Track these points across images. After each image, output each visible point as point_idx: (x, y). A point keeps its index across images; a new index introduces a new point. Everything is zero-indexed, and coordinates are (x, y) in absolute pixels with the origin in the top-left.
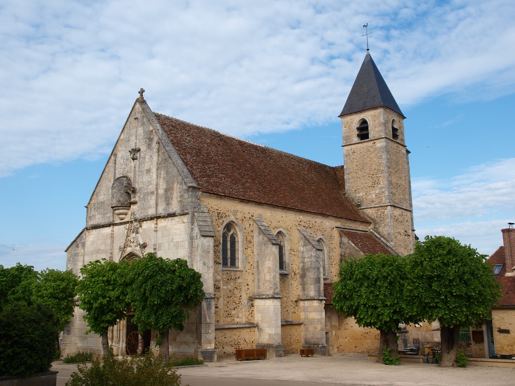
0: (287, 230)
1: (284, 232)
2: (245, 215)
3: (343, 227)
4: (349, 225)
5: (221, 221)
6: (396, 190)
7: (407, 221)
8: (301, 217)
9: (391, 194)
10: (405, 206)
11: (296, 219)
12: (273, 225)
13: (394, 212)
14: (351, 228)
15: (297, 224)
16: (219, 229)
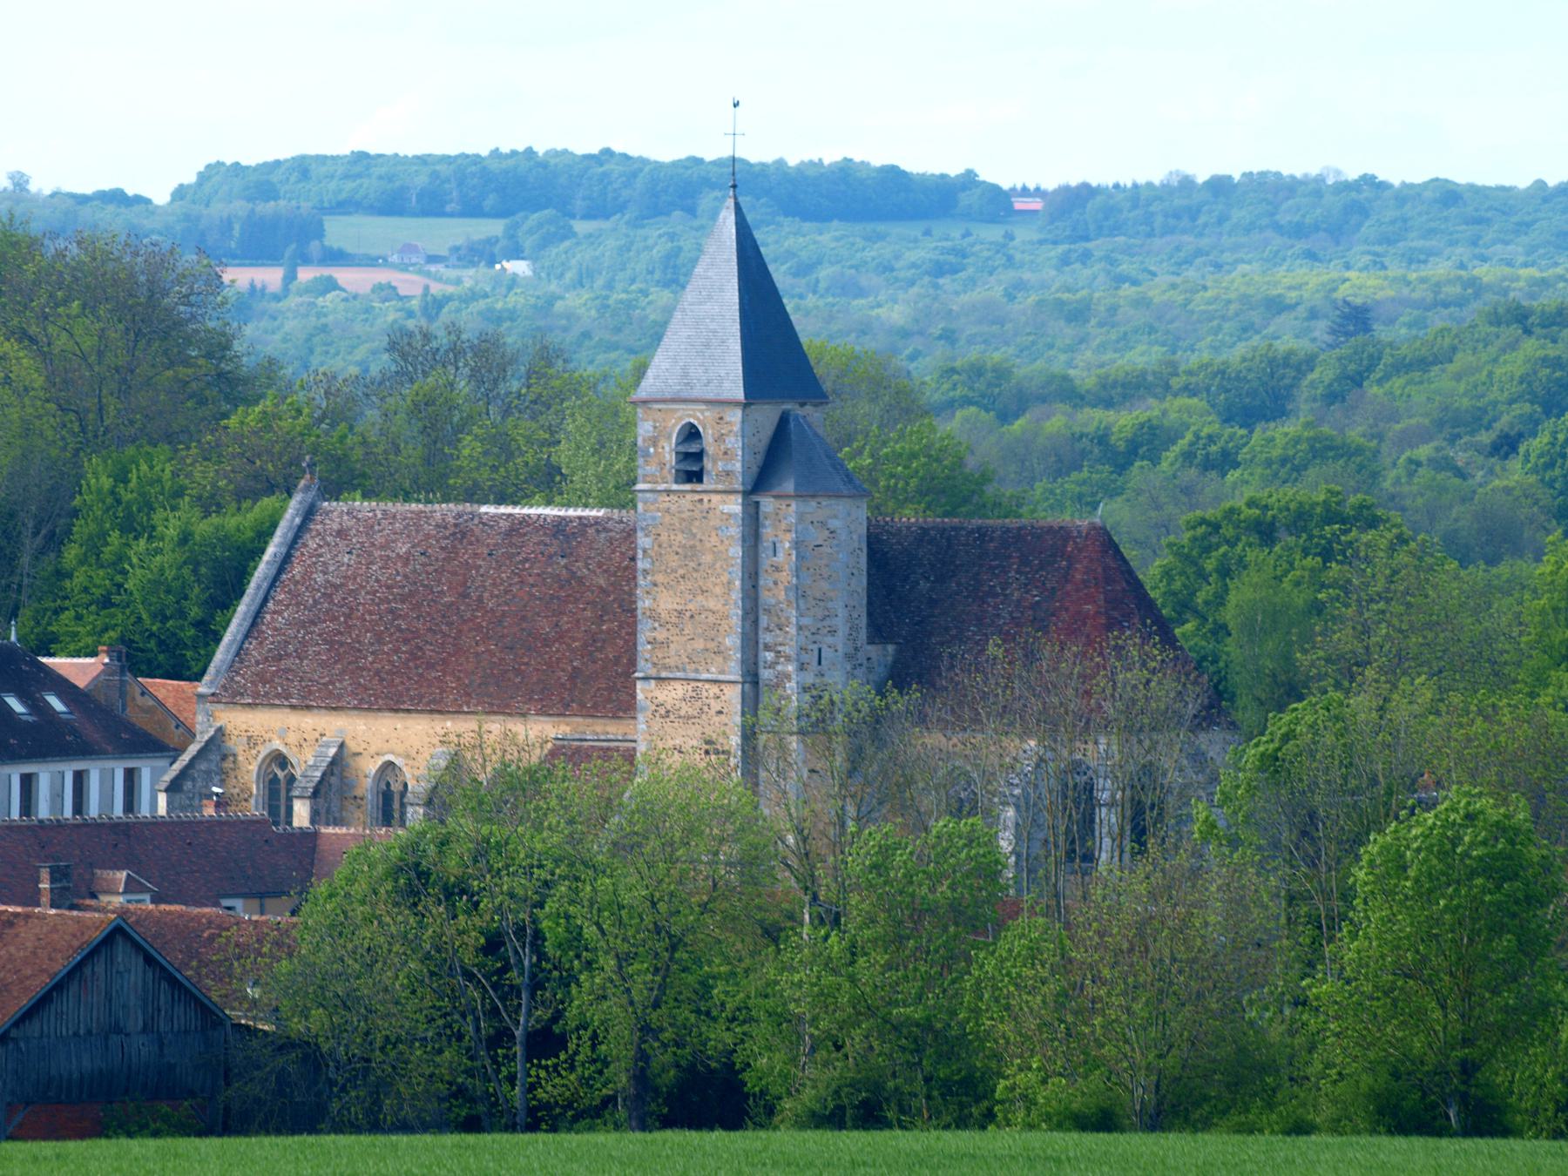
0: (408, 756)
1: (396, 762)
2: (305, 736)
3: (577, 736)
4: (599, 729)
5: (254, 752)
6: (674, 631)
7: (720, 712)
8: (449, 724)
9: (649, 647)
10: (713, 669)
11: (431, 731)
12: (373, 749)
13: (657, 693)
14: (603, 737)
15: (436, 741)
16: (251, 767)
